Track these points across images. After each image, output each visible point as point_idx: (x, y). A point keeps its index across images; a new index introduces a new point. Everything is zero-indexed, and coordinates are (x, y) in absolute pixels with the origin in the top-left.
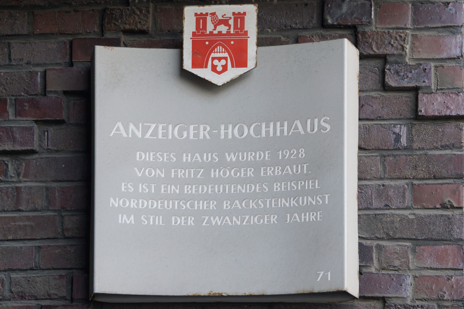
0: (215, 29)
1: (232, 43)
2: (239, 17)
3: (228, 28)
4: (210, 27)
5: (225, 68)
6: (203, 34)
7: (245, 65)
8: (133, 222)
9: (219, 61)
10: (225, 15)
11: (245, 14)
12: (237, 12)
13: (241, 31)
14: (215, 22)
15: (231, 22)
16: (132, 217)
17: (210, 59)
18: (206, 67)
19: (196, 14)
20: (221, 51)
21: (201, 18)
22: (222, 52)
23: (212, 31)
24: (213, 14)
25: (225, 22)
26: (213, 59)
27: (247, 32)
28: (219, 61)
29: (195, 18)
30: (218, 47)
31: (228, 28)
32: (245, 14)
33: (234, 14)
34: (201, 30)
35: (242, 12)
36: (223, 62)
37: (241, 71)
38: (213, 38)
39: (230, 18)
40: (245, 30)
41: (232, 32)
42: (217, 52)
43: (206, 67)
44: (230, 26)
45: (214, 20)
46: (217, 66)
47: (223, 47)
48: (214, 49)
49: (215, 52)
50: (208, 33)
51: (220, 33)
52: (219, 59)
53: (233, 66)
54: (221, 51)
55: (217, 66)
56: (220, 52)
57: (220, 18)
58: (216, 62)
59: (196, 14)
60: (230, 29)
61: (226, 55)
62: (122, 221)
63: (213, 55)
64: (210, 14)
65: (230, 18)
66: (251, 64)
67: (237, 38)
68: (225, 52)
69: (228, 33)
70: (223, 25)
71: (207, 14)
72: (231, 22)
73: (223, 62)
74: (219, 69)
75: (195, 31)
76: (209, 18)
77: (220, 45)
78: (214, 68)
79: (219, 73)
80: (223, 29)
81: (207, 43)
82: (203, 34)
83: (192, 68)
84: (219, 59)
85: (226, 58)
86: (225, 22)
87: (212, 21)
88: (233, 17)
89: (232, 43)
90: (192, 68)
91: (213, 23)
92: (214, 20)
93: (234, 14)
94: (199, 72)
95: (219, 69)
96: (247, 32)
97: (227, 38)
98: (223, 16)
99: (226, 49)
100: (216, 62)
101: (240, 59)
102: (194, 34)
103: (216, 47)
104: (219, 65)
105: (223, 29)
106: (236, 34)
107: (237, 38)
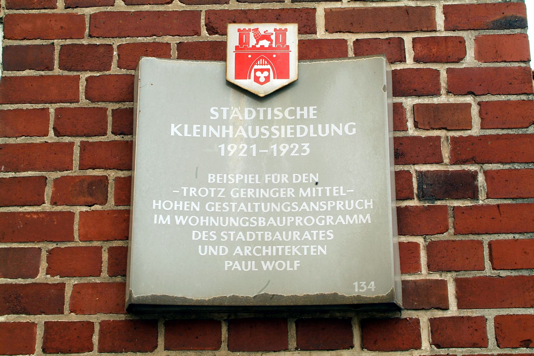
0: (257, 43)
1: (274, 56)
3: (270, 42)
4: (253, 42)
5: (267, 79)
7: (287, 76)
8: (169, 223)
10: (267, 31)
11: (286, 30)
12: (278, 29)
13: (283, 45)
14: (258, 37)
16: (169, 217)
18: (250, 78)
19: (239, 30)
22: (265, 65)
25: (267, 37)
26: (256, 70)
31: (270, 42)
32: (286, 30)
33: (275, 30)
34: (245, 44)
37: (284, 82)
38: (254, 52)
39: (272, 34)
41: (274, 46)
42: (260, 64)
44: (271, 41)
45: (256, 35)
46: (260, 77)
47: (265, 59)
49: (258, 65)
50: (251, 46)
51: (262, 47)
52: (262, 71)
53: (274, 78)
55: (260, 77)
56: (262, 65)
57: (262, 33)
58: (258, 74)
59: (239, 30)
60: (272, 43)
61: (269, 67)
62: (158, 221)
63: (256, 67)
64: (253, 30)
65: (272, 34)
66: (293, 75)
67: (278, 52)
68: (267, 65)
69: (270, 47)
70: (265, 40)
71: (250, 30)
72: (273, 37)
73: (266, 74)
74: (262, 80)
76: (252, 35)
77: (262, 58)
78: (257, 79)
79: (262, 84)
80: (265, 43)
84: (262, 71)
85: (268, 70)
86: (267, 37)
87: (254, 36)
88: (274, 33)
89: (274, 56)
91: (255, 38)
92: (256, 35)
93: (275, 30)
94: (241, 83)
95: (262, 80)
96: (288, 46)
98: (265, 32)
99: (268, 61)
100: (258, 74)
101: (282, 71)
102: (237, 48)
103: (259, 59)
104: (262, 76)
105: (265, 43)
107: (278, 52)
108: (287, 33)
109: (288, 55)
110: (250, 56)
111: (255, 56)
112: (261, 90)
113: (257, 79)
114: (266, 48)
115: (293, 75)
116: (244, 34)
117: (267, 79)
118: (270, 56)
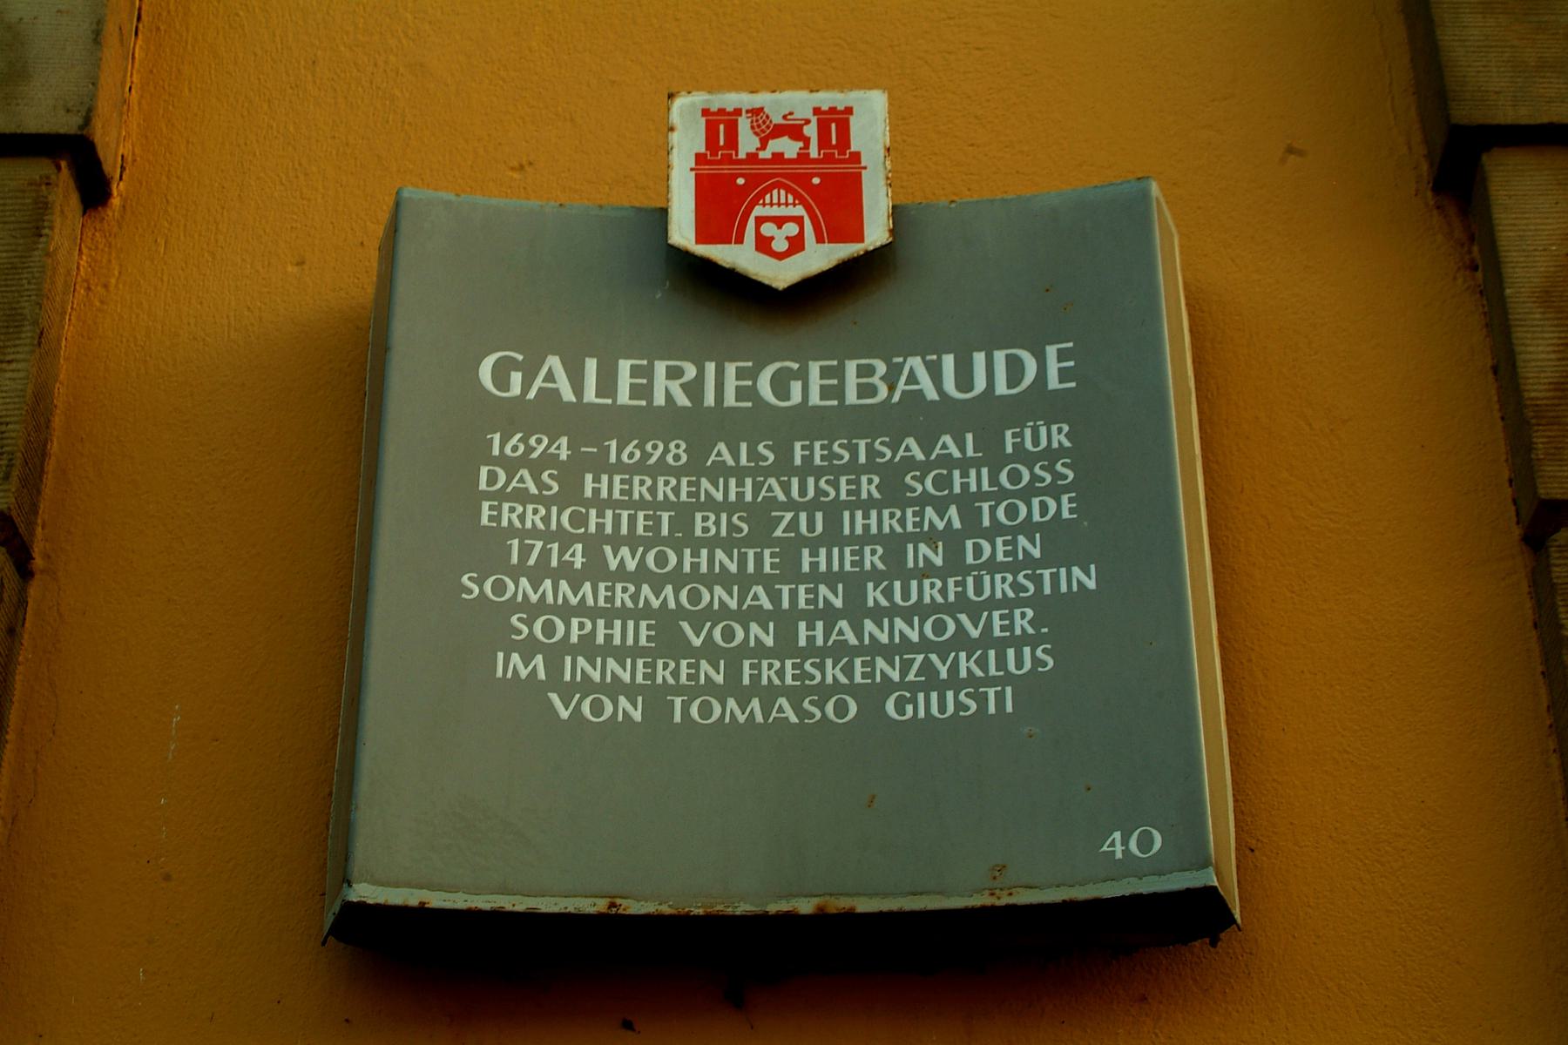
0: (763, 147)
1: (816, 181)
2: (836, 122)
3: (801, 144)
4: (747, 142)
5: (796, 244)
6: (728, 160)
9: (780, 227)
11: (849, 111)
15: (811, 131)
17: (751, 223)
18: (740, 240)
19: (705, 112)
20: (783, 200)
21: (720, 125)
22: (787, 204)
23: (753, 150)
24: (756, 112)
25: (795, 131)
26: (760, 221)
27: (856, 157)
28: (780, 227)
29: (703, 120)
30: (775, 192)
31: (801, 144)
32: (849, 111)
33: (817, 111)
34: (722, 148)
35: (841, 107)
36: (791, 229)
39: (808, 122)
40: (853, 148)
41: (814, 152)
42: (772, 204)
43: (740, 240)
44: (807, 141)
46: (772, 238)
47: (789, 190)
48: (761, 195)
50: (742, 155)
51: (778, 157)
52: (780, 221)
53: (820, 240)
54: (783, 200)
55: (772, 238)
56: (779, 204)
57: (777, 119)
58: (768, 229)
59: (705, 112)
60: (807, 145)
61: (799, 211)
63: (758, 211)
69: (803, 157)
71: (738, 112)
74: (780, 245)
75: (703, 150)
76: (744, 124)
77: (779, 186)
78: (763, 245)
79: (780, 256)
80: (788, 147)
81: (741, 181)
82: (728, 160)
83: (698, 241)
84: (780, 221)
85: (799, 220)
88: (814, 120)
89: (816, 181)
90: (698, 241)
93: (817, 111)
95: (780, 245)
97: (801, 169)
98: (785, 117)
99: (796, 196)
102: (700, 158)
103: (769, 190)
105: (788, 147)
106: (828, 159)
108: (853, 119)
109: (857, 179)
110: (741, 181)
111: (754, 181)
112: (781, 274)
113: (763, 245)
114: (790, 161)
115: (876, 233)
116: (720, 122)
117: (796, 244)
118: (803, 180)
